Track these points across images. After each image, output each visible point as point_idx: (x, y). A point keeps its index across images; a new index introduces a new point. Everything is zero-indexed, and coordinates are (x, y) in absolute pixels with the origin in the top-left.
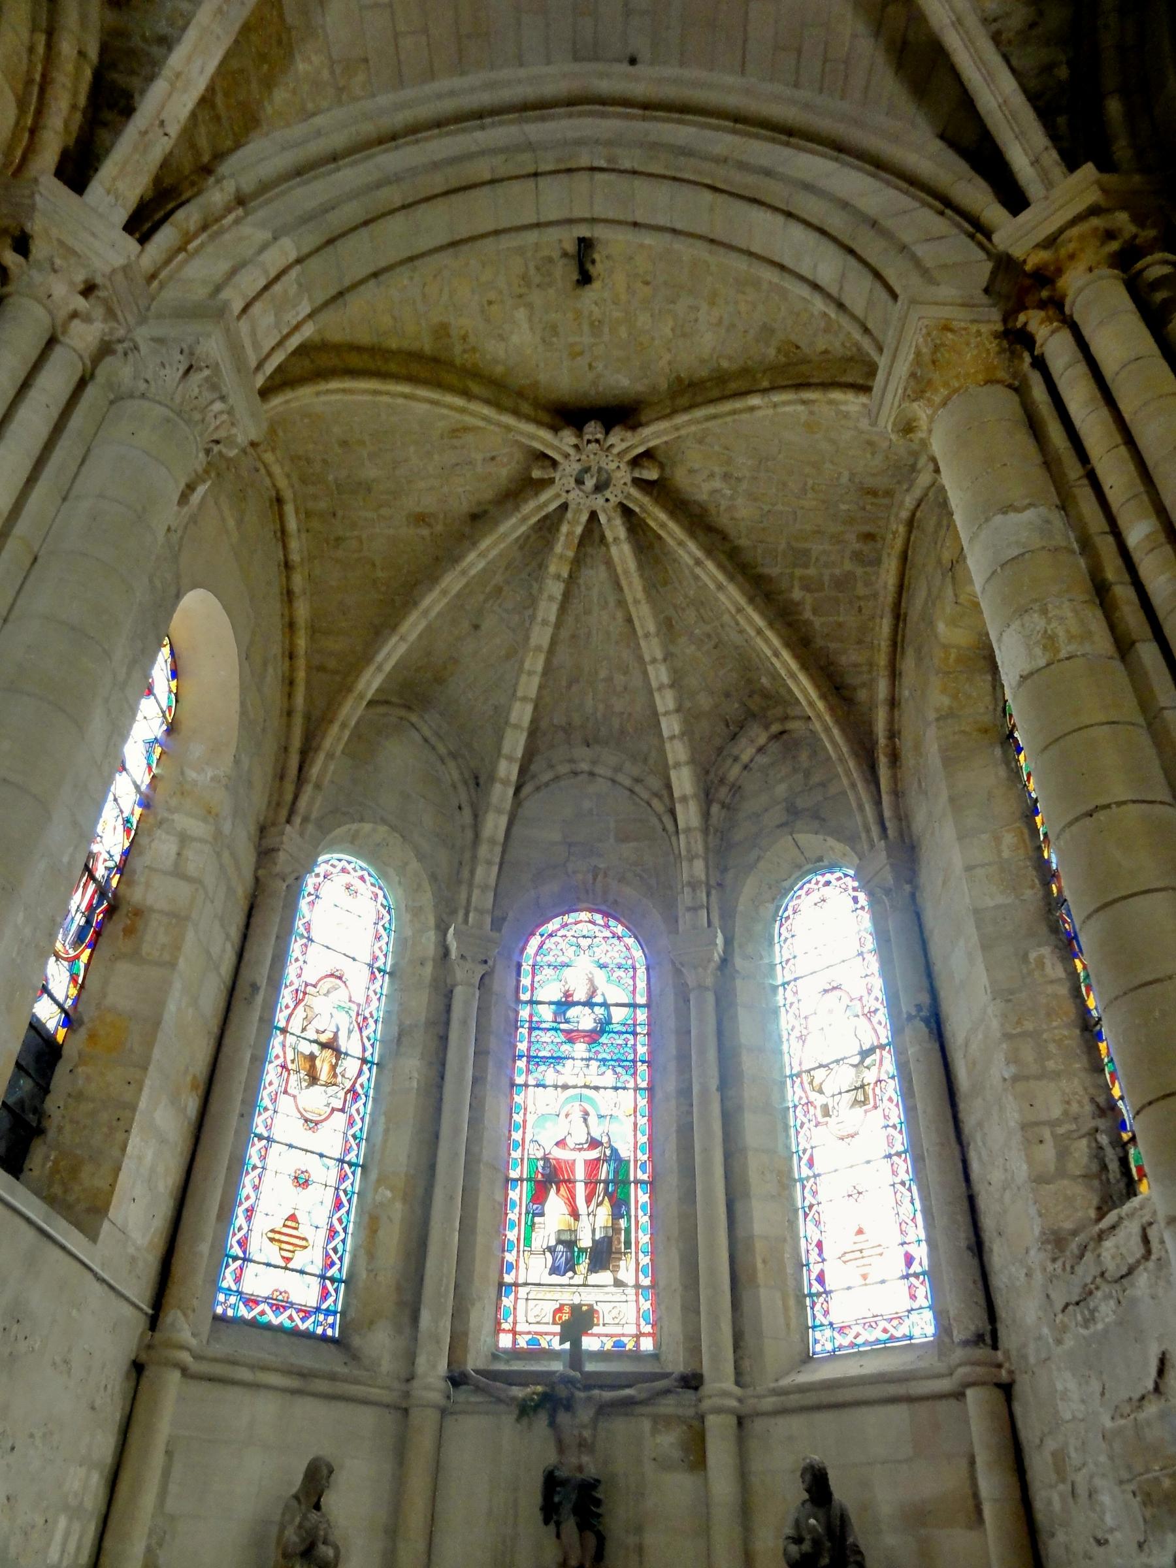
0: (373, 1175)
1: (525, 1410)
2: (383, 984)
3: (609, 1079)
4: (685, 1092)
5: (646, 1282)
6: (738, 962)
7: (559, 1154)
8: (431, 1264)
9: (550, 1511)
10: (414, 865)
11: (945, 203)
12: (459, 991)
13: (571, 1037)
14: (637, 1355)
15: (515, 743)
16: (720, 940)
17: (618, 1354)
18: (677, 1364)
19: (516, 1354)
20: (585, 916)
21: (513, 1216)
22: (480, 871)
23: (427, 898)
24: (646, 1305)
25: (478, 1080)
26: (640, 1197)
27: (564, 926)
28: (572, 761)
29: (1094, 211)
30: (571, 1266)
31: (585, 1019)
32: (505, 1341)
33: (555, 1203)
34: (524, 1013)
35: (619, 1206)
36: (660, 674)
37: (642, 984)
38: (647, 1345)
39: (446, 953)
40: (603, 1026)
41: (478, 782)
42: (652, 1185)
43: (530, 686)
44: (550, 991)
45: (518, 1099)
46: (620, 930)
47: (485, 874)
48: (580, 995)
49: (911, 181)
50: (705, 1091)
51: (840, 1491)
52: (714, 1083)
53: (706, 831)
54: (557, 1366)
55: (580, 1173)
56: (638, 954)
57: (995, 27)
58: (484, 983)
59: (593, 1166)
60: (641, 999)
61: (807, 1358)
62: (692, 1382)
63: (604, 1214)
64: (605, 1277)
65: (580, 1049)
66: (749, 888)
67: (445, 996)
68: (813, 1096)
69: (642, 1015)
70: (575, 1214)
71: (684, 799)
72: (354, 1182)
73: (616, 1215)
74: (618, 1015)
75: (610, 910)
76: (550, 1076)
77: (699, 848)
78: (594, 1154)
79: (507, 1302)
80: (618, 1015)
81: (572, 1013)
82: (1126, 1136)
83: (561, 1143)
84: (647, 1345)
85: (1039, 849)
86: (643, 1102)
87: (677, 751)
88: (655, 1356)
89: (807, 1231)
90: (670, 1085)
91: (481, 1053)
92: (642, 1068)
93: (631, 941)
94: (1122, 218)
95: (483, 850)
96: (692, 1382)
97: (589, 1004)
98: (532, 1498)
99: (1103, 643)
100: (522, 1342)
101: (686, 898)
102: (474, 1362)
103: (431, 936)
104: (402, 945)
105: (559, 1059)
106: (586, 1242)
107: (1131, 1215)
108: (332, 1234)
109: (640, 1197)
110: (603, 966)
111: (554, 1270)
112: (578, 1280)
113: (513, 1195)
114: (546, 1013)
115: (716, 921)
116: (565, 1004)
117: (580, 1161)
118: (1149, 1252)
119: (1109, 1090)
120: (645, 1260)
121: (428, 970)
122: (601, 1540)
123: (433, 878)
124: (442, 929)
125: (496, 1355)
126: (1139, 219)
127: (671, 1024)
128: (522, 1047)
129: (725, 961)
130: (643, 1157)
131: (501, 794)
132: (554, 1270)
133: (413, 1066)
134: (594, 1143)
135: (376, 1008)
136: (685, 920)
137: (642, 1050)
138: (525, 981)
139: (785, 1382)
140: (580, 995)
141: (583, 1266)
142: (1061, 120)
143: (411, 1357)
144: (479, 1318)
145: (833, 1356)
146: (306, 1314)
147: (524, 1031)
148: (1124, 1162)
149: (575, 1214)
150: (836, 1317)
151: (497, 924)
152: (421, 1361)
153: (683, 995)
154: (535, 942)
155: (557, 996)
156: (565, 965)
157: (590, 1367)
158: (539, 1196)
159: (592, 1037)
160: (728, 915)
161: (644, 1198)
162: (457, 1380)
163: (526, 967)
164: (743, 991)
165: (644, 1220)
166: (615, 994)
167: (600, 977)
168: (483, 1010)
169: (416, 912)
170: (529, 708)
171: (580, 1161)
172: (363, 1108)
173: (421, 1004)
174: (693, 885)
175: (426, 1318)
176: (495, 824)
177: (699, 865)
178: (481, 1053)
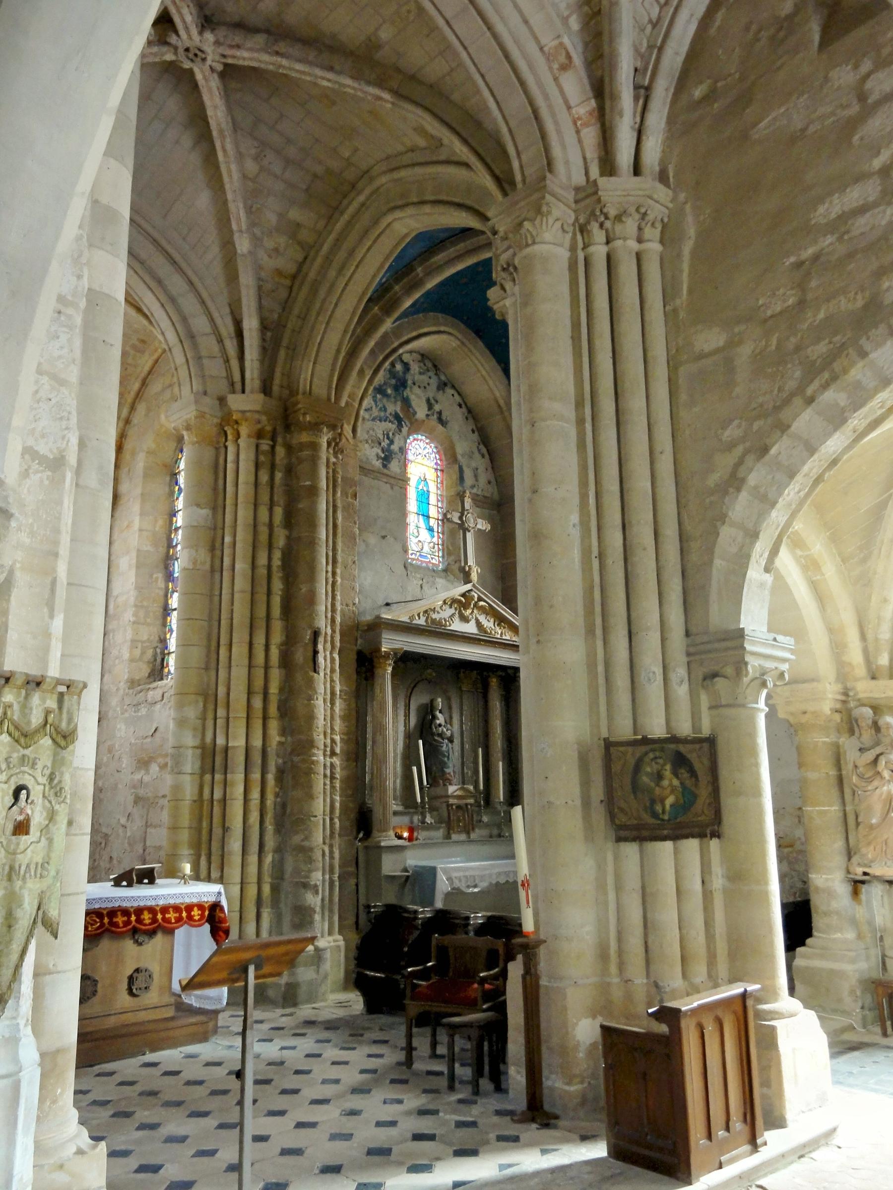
11: (220, 341)
29: (258, 412)
49: (212, 320)
57: (261, 283)
82: (166, 652)
85: (171, 533)
94: (264, 418)
99: (207, 566)
107: (161, 687)
118: (163, 699)
119: (165, 634)
126: (269, 420)
142: (269, 334)
148: (163, 660)
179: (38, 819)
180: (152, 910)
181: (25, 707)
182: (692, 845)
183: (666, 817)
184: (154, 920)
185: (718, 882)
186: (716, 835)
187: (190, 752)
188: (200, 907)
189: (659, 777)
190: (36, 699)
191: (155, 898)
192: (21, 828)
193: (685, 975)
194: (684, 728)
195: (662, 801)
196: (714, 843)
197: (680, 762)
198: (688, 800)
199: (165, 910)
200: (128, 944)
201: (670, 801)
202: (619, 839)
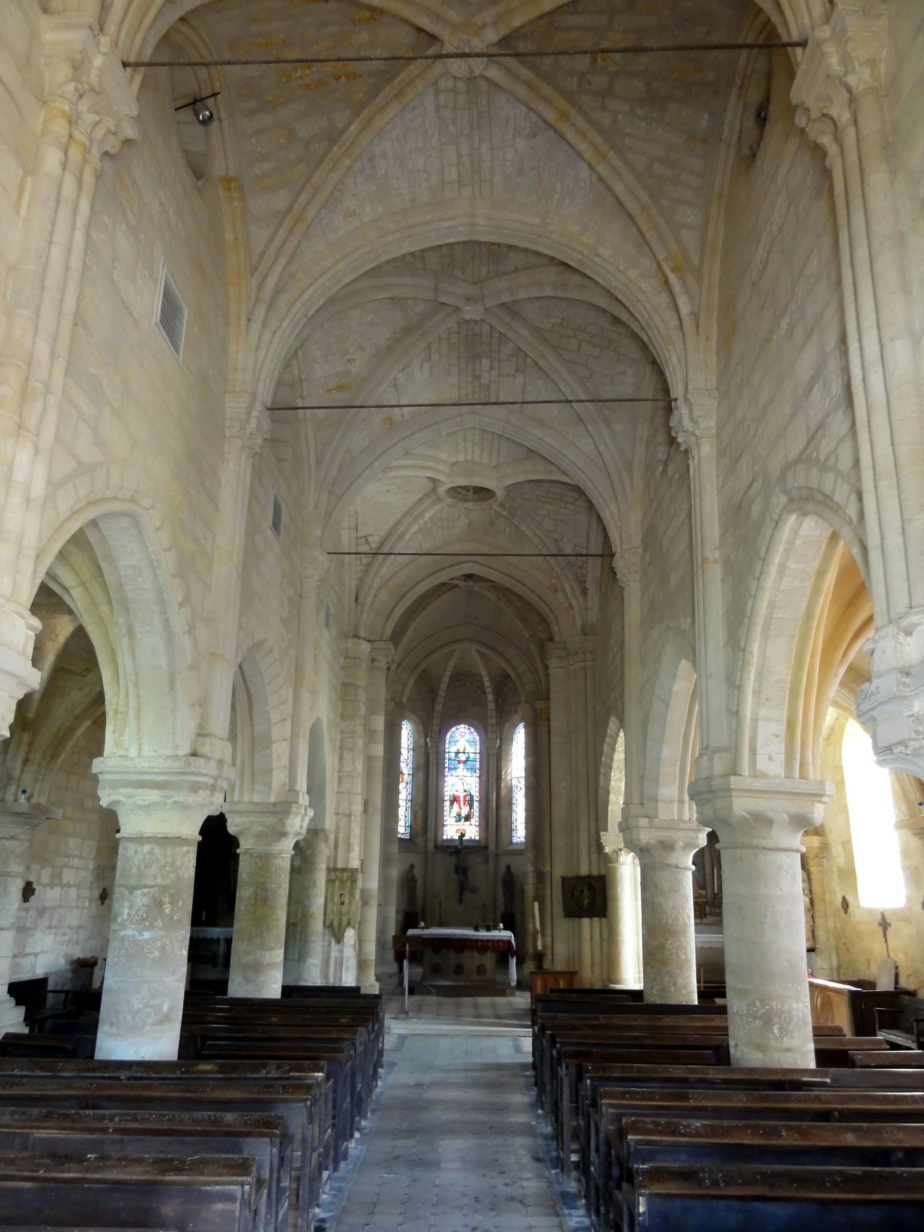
0: (414, 803)
1: (451, 854)
2: (411, 752)
3: (469, 774)
4: (488, 781)
5: (478, 824)
6: (503, 747)
7: (457, 794)
8: (429, 825)
9: (457, 872)
10: (418, 720)
12: (431, 755)
13: (459, 762)
14: (474, 841)
15: (444, 686)
16: (498, 743)
17: (471, 840)
18: (483, 844)
19: (447, 840)
20: (463, 726)
21: (445, 809)
22: (435, 720)
23: (421, 729)
24: (477, 829)
25: (437, 778)
26: (476, 804)
27: (457, 729)
28: (460, 681)
30: (460, 820)
31: (462, 757)
32: (445, 837)
33: (456, 805)
34: (447, 755)
35: (471, 806)
36: (484, 673)
37: (478, 747)
38: (477, 838)
39: (426, 744)
40: (467, 760)
41: (433, 691)
42: (480, 802)
43: (448, 673)
44: (453, 749)
45: (446, 779)
46: (472, 730)
47: (436, 721)
48: (461, 750)
50: (492, 783)
51: (513, 869)
52: (495, 781)
53: (496, 708)
54: (457, 843)
55: (462, 799)
56: (477, 738)
58: (437, 753)
59: (465, 797)
60: (478, 751)
61: (511, 843)
62: (486, 848)
63: (467, 808)
64: (468, 823)
65: (462, 765)
66: (507, 726)
67: (427, 755)
68: (518, 784)
69: (478, 756)
70: (460, 808)
71: (490, 702)
72: (409, 804)
73: (471, 809)
74: (472, 756)
75: (471, 725)
76: (453, 772)
77: (494, 714)
78: (465, 794)
79: (445, 828)
80: (472, 756)
81: (459, 755)
83: (457, 791)
84: (477, 838)
86: (478, 780)
87: (489, 690)
88: (478, 841)
89: (514, 815)
90: (484, 778)
91: (437, 770)
92: (478, 771)
93: (475, 734)
95: (436, 715)
96: (486, 848)
97: (464, 753)
98: (453, 869)
100: (449, 838)
101: (490, 728)
102: (439, 843)
103: (422, 740)
104: (415, 742)
105: (456, 769)
106: (463, 815)
108: (406, 817)
109: (476, 804)
110: (468, 741)
111: (456, 821)
112: (462, 823)
113: (445, 804)
114: (453, 755)
115: (498, 735)
116: (457, 753)
117: (461, 795)
120: (477, 819)
121: (422, 750)
122: (467, 877)
123: (422, 722)
124: (426, 737)
125: (444, 841)
127: (485, 762)
128: (447, 765)
129: (500, 747)
130: (478, 794)
131: (440, 699)
132: (456, 821)
133: (421, 776)
134: (465, 791)
135: (411, 759)
136: (490, 735)
137: (478, 766)
138: (447, 746)
139: (507, 848)
140: (461, 750)
141: (463, 820)
143: (426, 842)
144: (439, 833)
145: (517, 844)
146: (403, 834)
147: (447, 761)
149: (460, 808)
150: (518, 836)
151: (440, 732)
152: (428, 844)
153: (488, 755)
154: (449, 733)
155: (456, 751)
156: (457, 741)
157: (465, 844)
158: (452, 804)
159: (465, 762)
160: (501, 733)
161: (478, 804)
162: (436, 847)
163: (447, 742)
164: (503, 754)
165: (477, 810)
166: (470, 749)
167: (467, 745)
168: (437, 759)
169: (418, 733)
170: (448, 679)
171: (461, 795)
172: (410, 786)
173: (422, 760)
174: (492, 725)
175: (429, 835)
176: (439, 708)
177: (494, 721)
178: (437, 770)
179: (347, 900)
180: (482, 941)
181: (342, 876)
182: (596, 920)
183: (585, 908)
184: (483, 945)
185: (605, 936)
186: (605, 916)
187: (531, 874)
188: (503, 941)
189: (582, 892)
190: (345, 874)
191: (484, 936)
192: (342, 903)
193: (592, 972)
194: (595, 872)
195: (583, 902)
196: (604, 919)
197: (590, 887)
198: (593, 901)
199: (488, 941)
200: (476, 954)
201: (586, 902)
202: (565, 916)
